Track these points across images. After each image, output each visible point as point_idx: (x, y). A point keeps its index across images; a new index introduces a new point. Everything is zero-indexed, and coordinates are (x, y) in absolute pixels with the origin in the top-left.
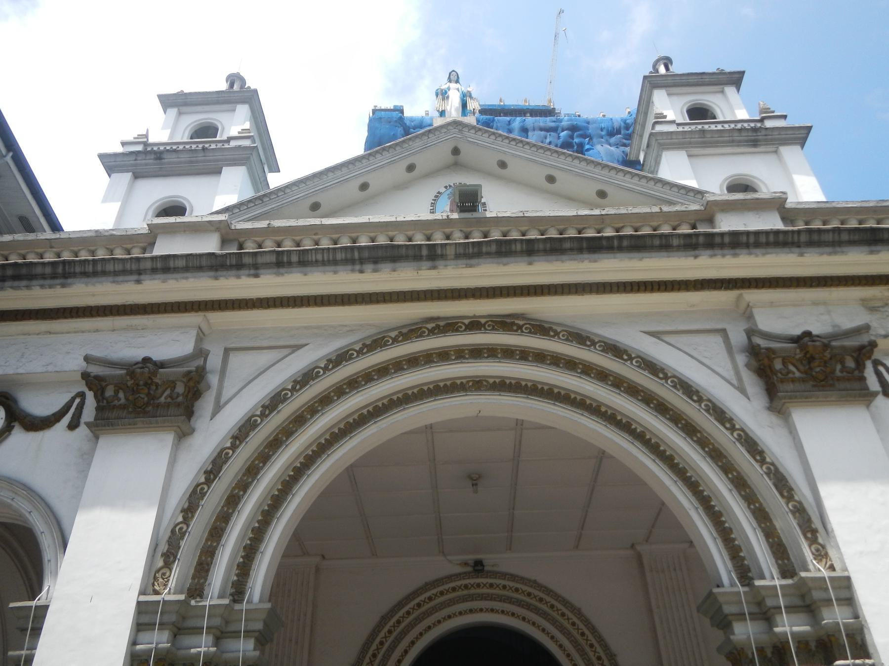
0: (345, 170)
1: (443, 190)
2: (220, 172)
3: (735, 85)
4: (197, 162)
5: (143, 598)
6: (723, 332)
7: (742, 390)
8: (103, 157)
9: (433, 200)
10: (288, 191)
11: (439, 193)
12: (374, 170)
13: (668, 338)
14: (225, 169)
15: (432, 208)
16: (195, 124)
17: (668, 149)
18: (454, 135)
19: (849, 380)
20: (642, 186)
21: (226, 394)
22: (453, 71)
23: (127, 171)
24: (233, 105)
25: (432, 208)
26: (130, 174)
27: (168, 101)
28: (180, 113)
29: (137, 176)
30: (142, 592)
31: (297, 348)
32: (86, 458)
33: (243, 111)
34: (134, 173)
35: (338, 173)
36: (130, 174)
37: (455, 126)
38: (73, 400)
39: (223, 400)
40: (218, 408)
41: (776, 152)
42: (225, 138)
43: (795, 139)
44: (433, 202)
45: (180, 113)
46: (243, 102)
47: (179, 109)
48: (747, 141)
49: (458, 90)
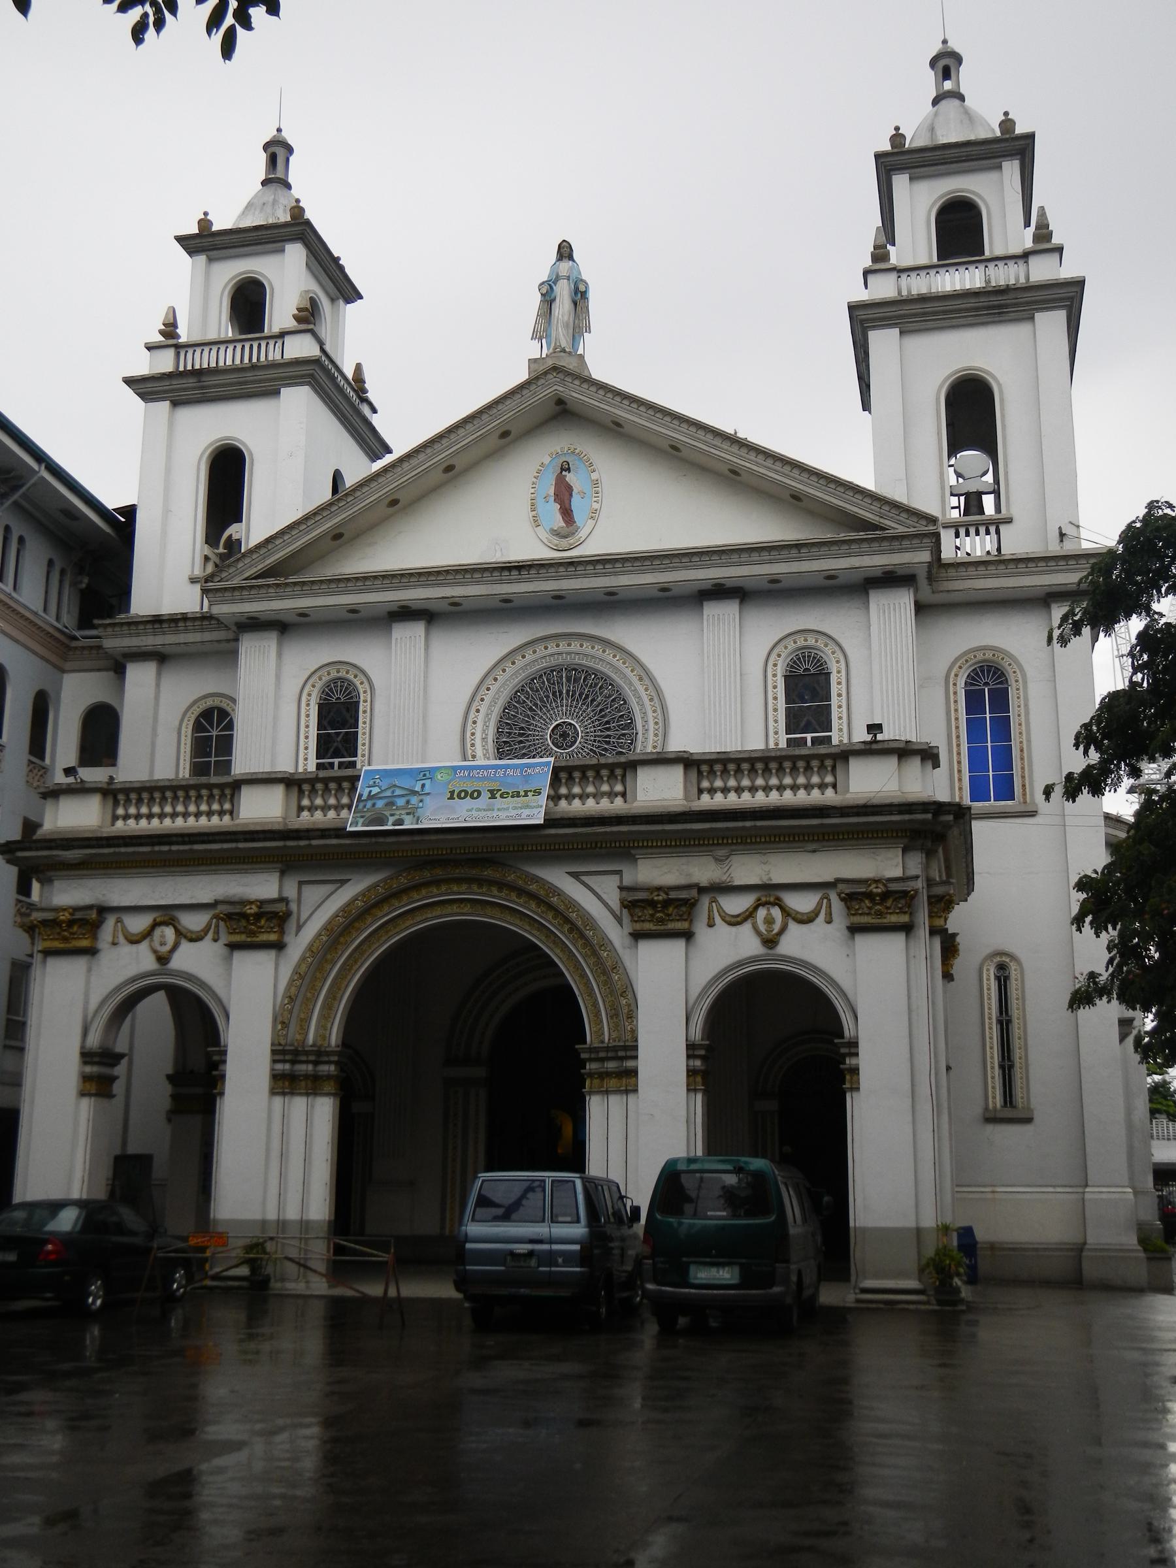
0: (422, 457)
1: (547, 460)
2: (276, 393)
3: (1019, 157)
4: (245, 383)
5: (274, 1048)
6: (619, 872)
7: (619, 920)
8: (130, 382)
9: (535, 477)
10: (358, 493)
11: (542, 465)
12: (457, 453)
13: (583, 878)
14: (282, 389)
15: (533, 490)
16: (234, 281)
17: (874, 328)
18: (556, 387)
19: (678, 920)
20: (776, 472)
21: (303, 917)
22: (564, 241)
23: (163, 399)
24: (280, 244)
25: (533, 490)
26: (167, 403)
27: (191, 244)
28: (210, 260)
29: (175, 404)
30: (272, 1045)
31: (343, 882)
32: (228, 960)
33: (295, 253)
34: (171, 401)
35: (414, 462)
36: (167, 403)
37: (555, 374)
38: (212, 919)
39: (302, 920)
40: (299, 928)
41: (1032, 318)
42: (276, 329)
43: (1061, 300)
44: (535, 480)
45: (210, 260)
46: (293, 239)
47: (207, 256)
48: (988, 308)
49: (568, 278)
